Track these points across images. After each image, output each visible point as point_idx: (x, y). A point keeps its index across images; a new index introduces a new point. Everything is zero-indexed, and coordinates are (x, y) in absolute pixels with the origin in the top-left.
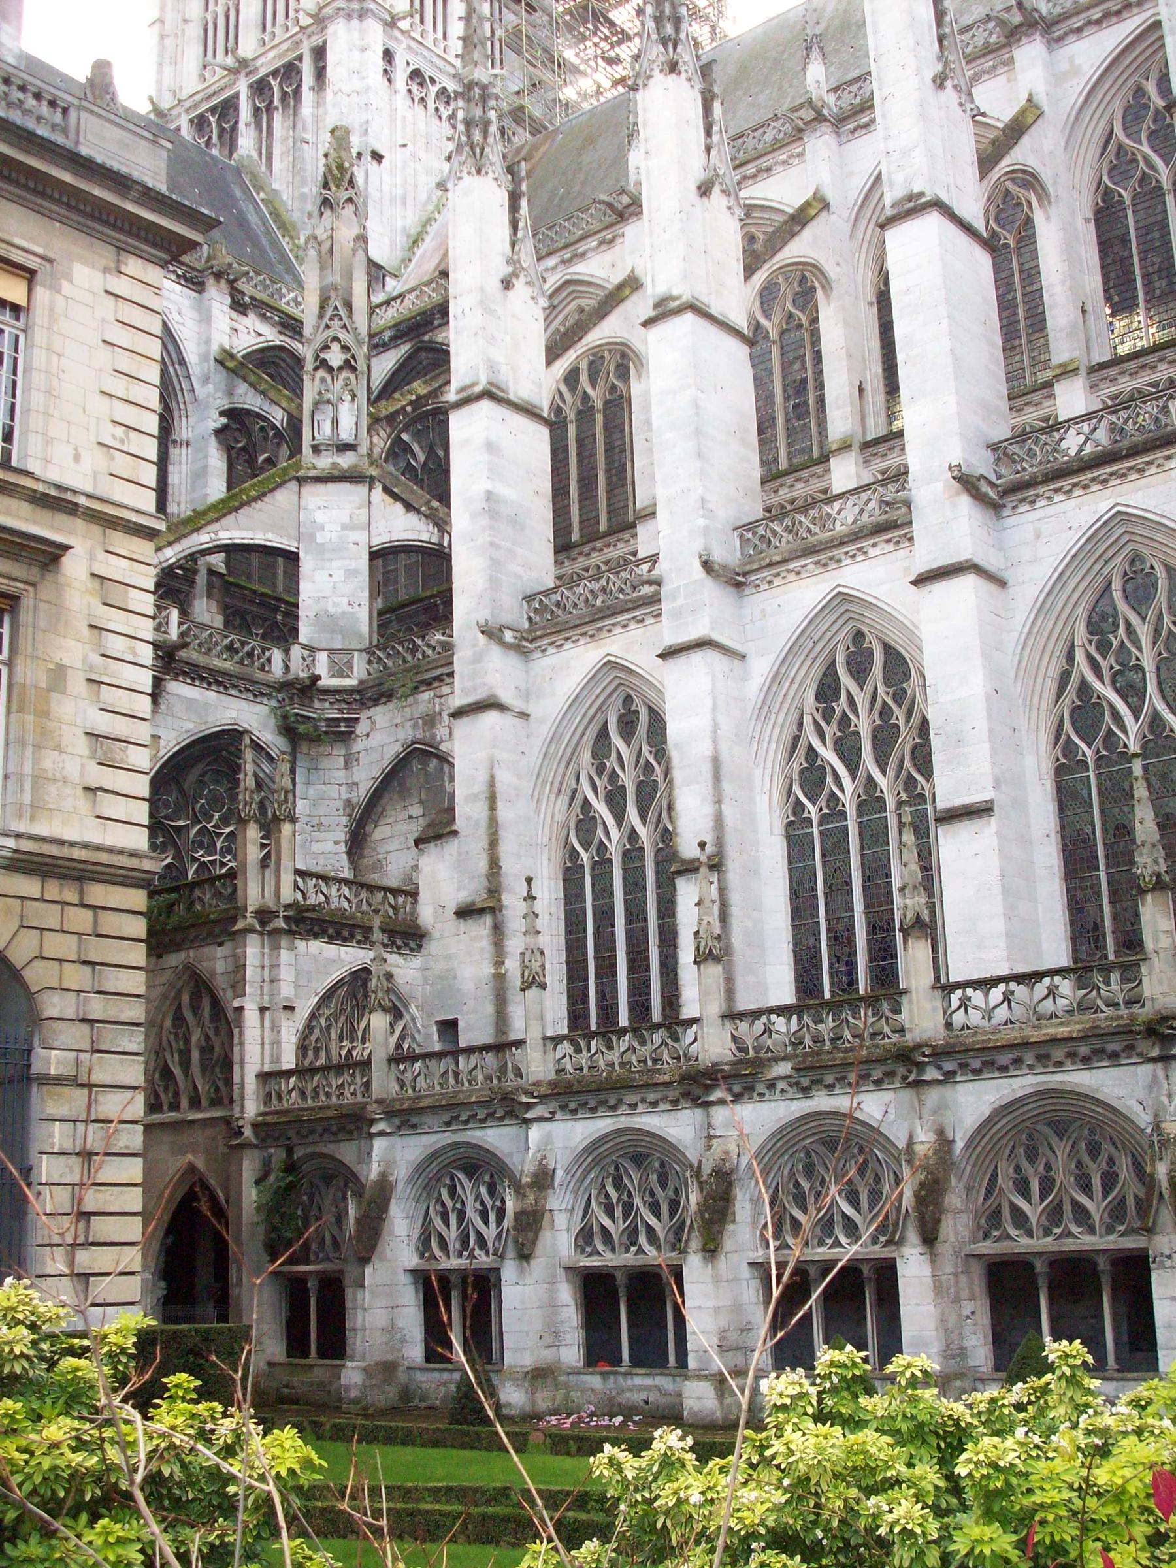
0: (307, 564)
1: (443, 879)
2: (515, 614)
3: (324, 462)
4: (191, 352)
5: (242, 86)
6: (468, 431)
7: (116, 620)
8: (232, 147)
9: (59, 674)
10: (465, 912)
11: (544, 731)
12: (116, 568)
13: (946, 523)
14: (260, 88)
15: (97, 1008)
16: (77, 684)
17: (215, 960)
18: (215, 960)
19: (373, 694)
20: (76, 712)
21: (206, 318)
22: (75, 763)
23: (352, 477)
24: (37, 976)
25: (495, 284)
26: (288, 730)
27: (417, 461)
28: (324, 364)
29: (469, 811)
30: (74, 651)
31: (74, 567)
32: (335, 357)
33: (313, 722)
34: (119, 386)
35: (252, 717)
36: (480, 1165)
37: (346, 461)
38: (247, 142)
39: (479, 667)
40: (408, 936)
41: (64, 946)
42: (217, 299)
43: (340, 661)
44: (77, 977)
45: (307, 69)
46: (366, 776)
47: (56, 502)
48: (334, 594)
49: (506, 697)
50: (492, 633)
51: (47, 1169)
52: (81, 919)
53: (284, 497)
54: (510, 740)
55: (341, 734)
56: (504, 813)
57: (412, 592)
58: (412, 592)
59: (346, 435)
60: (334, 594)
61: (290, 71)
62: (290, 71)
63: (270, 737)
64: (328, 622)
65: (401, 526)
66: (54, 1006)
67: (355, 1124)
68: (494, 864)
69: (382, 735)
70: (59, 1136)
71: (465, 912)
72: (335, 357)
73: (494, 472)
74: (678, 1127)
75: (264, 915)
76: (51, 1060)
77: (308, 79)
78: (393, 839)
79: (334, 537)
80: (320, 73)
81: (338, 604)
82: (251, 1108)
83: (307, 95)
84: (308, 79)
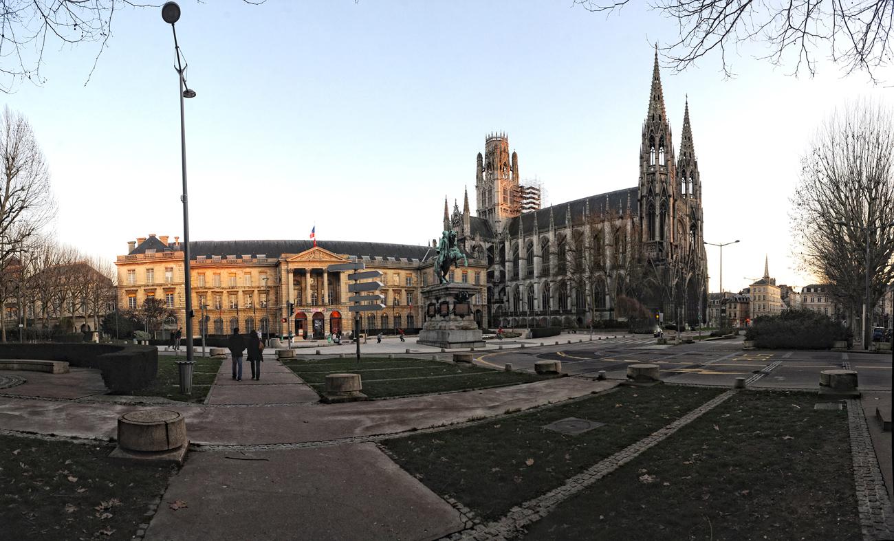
1: (505, 298)
6: (507, 264)
13: (536, 280)
19: (500, 283)
26: (494, 286)
27: (503, 263)
36: (506, 319)
38: (487, 216)
40: (503, 302)
46: (500, 289)
48: (497, 273)
54: (510, 286)
57: (503, 274)
58: (503, 274)
60: (497, 273)
61: (491, 209)
62: (491, 209)
65: (502, 269)
67: (499, 317)
74: (517, 318)
78: (502, 294)
79: (497, 268)
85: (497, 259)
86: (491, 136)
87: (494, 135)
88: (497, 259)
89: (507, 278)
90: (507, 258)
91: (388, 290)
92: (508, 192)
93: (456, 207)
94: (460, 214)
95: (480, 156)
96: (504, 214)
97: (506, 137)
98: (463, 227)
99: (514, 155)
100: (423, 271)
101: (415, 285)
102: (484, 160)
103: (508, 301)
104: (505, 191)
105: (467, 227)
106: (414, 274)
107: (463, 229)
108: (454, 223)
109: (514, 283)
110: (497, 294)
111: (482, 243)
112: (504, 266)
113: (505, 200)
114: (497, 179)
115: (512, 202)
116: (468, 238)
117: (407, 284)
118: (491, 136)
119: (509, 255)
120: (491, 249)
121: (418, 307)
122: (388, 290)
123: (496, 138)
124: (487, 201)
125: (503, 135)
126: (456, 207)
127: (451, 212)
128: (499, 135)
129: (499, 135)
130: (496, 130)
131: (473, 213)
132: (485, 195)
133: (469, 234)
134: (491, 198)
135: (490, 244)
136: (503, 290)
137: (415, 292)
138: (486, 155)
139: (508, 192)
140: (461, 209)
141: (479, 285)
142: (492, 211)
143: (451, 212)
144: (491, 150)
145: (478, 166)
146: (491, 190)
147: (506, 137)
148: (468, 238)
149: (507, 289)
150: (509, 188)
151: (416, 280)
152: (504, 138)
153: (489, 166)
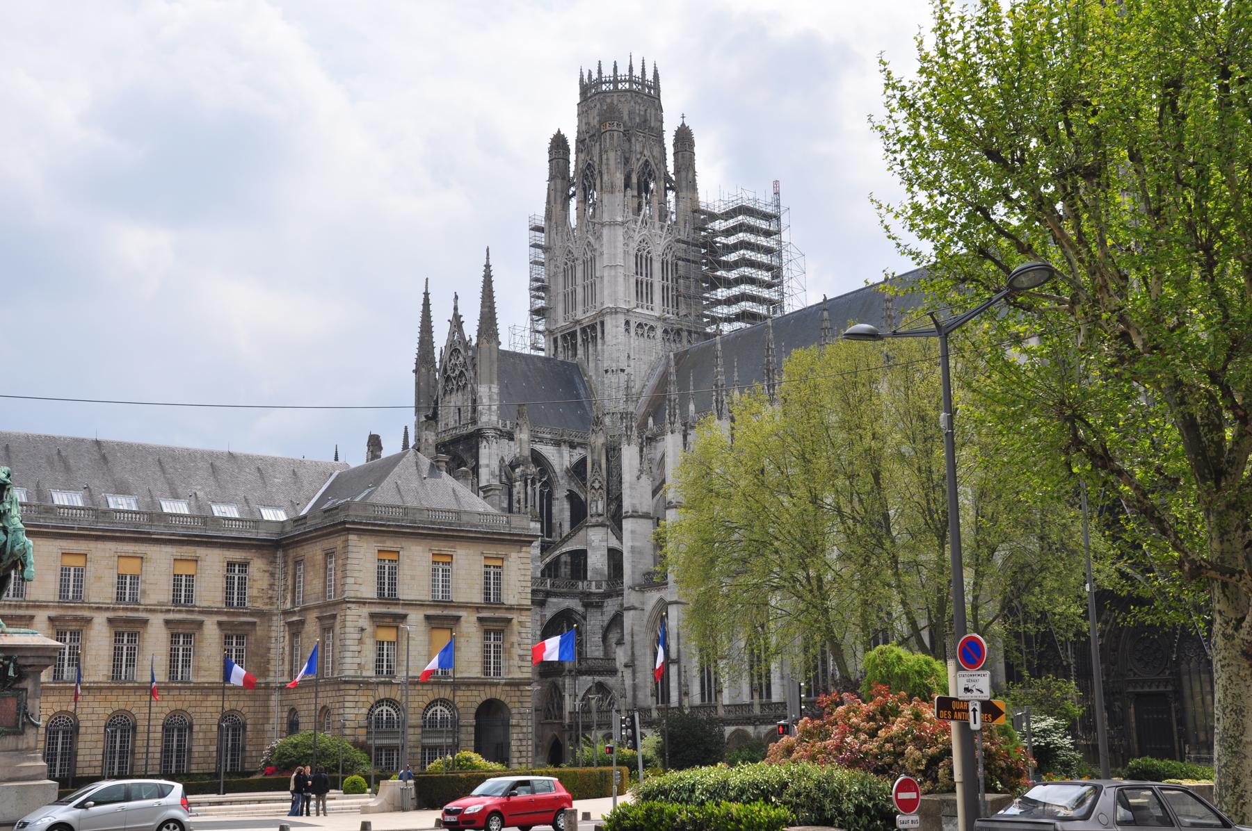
0: (589, 553)
1: (621, 656)
2: (639, 579)
3: (594, 520)
4: (557, 470)
5: (578, 328)
6: (627, 525)
7: (523, 630)
8: (576, 354)
9: (512, 644)
10: (626, 666)
11: (647, 614)
12: (523, 619)
14: (584, 330)
15: (522, 710)
16: (516, 645)
17: (560, 681)
18: (560, 681)
20: (517, 651)
21: (561, 456)
22: (516, 662)
23: (602, 525)
24: (510, 706)
25: (635, 478)
26: (586, 606)
28: (593, 487)
29: (627, 638)
30: (515, 639)
31: (515, 621)
32: (597, 485)
33: (592, 602)
34: (522, 567)
35: (574, 604)
37: (600, 519)
38: (580, 352)
39: (630, 598)
40: (613, 672)
41: (516, 699)
42: (565, 450)
43: (598, 587)
44: (517, 705)
45: (599, 327)
47: (510, 608)
48: (597, 561)
49: (637, 605)
50: (632, 588)
51: (513, 743)
52: (518, 693)
53: (581, 533)
55: (599, 606)
56: (636, 638)
59: (600, 511)
61: (593, 327)
62: (593, 327)
63: (580, 609)
64: (596, 571)
65: (614, 543)
66: (514, 711)
68: (633, 653)
69: (611, 607)
70: (515, 736)
71: (626, 666)
72: (597, 485)
73: (633, 540)
75: (570, 671)
76: (513, 722)
77: (599, 335)
79: (596, 542)
80: (603, 333)
81: (599, 565)
82: (567, 721)
83: (599, 341)
84: (599, 335)
85: (598, 506)
86: (595, 76)
87: (608, 72)
88: (598, 506)
89: (627, 579)
90: (627, 506)
91: (145, 622)
92: (657, 266)
93: (457, 322)
94: (467, 345)
95: (559, 143)
96: (635, 342)
97: (649, 76)
98: (474, 392)
99: (684, 138)
100: (292, 553)
101: (259, 605)
102: (572, 157)
103: (631, 665)
104: (642, 261)
105: (488, 393)
106: (258, 567)
107: (474, 401)
108: (448, 379)
109: (653, 597)
110: (597, 638)
111: (548, 451)
112: (618, 531)
113: (643, 290)
114: (613, 224)
115: (675, 297)
116: (491, 433)
117: (229, 603)
118: (595, 76)
119: (635, 494)
120: (578, 470)
121: (267, 686)
122: (145, 622)
123: (616, 81)
124: (580, 297)
125: (637, 72)
126: (457, 322)
127: (440, 339)
128: (623, 71)
129: (623, 71)
130: (611, 55)
131: (517, 332)
132: (574, 277)
133: (494, 418)
134: (593, 285)
135: (578, 454)
136: (617, 620)
137: (259, 631)
138: (580, 141)
139: (657, 266)
140: (471, 330)
141: (499, 605)
142: (592, 332)
143: (440, 339)
144: (595, 122)
145: (552, 178)
146: (593, 259)
147: (649, 76)
148: (491, 433)
149: (628, 618)
150: (659, 246)
151: (264, 584)
152: (643, 82)
153: (589, 176)
